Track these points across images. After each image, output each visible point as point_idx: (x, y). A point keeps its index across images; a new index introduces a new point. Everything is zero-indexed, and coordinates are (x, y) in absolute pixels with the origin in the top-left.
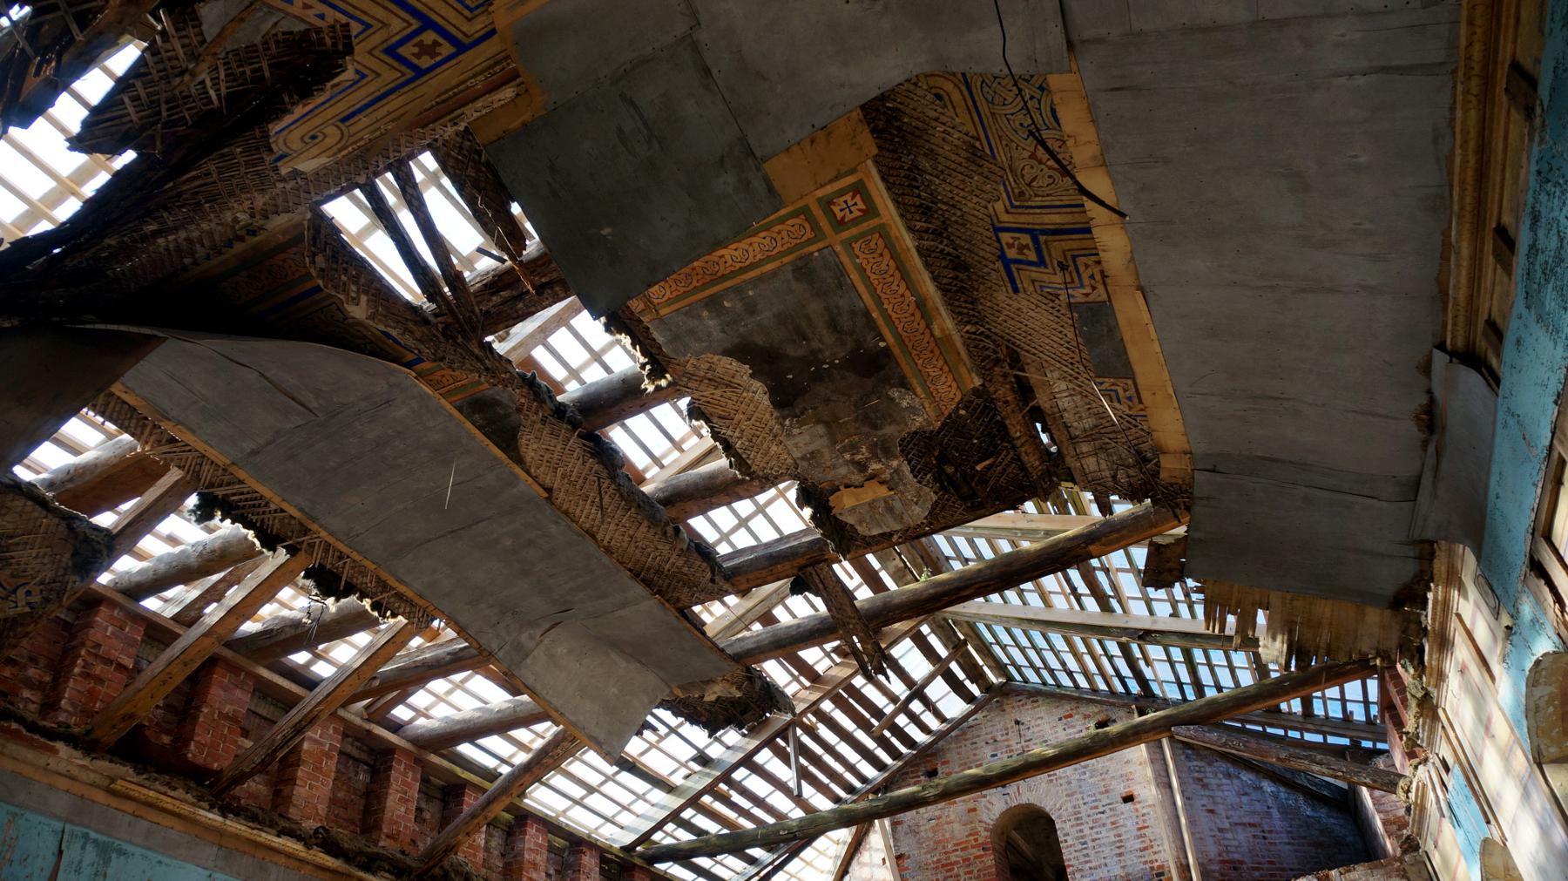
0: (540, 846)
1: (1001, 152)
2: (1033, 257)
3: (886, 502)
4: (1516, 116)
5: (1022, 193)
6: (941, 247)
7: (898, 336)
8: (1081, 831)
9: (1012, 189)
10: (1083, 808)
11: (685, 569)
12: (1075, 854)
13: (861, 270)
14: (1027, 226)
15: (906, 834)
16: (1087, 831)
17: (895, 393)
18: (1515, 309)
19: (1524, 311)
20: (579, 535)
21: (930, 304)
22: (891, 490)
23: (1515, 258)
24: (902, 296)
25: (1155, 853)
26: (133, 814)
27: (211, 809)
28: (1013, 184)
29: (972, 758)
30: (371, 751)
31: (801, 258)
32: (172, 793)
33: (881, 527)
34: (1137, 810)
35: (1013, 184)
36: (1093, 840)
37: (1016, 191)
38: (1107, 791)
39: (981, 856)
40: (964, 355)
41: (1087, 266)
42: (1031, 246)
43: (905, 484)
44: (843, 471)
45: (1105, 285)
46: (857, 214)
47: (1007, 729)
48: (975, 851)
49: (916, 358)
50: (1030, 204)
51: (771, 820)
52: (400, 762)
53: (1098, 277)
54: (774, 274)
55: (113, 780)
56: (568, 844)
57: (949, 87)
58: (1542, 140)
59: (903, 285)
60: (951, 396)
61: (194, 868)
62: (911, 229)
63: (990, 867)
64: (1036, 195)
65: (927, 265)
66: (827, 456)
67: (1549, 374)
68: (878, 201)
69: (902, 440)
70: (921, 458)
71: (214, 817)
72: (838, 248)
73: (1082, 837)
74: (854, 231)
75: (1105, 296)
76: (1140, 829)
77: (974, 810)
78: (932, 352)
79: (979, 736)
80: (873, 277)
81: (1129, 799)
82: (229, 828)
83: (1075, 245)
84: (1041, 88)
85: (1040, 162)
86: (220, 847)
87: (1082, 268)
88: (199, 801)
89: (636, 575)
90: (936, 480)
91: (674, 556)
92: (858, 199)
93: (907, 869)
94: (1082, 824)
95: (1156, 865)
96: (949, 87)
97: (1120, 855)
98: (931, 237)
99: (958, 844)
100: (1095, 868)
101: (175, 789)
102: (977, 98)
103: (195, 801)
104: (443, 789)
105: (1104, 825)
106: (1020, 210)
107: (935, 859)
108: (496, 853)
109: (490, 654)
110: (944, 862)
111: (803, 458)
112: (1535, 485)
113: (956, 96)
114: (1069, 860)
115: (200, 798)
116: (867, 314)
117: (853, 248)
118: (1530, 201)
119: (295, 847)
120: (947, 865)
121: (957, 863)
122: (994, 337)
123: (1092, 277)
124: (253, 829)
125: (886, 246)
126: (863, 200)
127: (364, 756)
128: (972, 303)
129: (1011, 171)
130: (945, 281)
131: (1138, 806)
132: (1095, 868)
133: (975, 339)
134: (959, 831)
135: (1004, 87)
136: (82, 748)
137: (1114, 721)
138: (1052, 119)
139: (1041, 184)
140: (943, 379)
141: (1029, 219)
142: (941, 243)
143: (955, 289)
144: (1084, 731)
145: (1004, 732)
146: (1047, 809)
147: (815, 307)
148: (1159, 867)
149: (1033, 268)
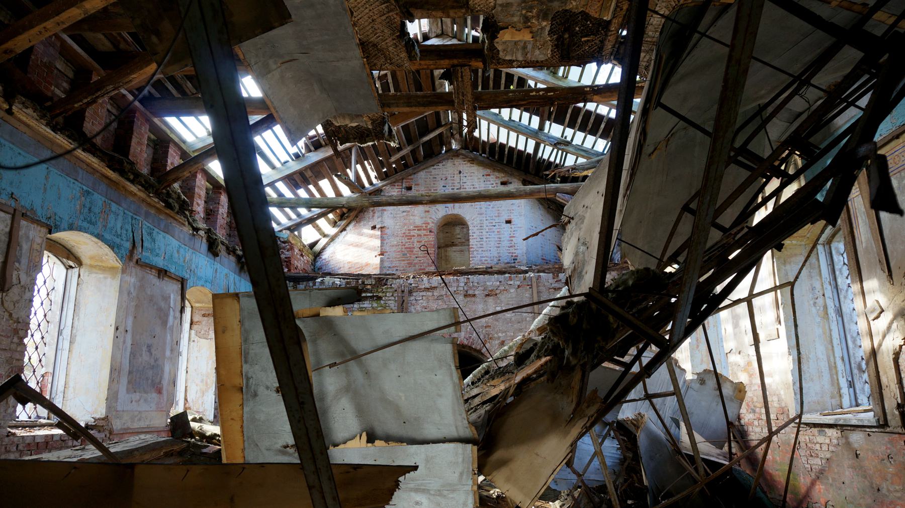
3: (525, 43)
8: (482, 232)
10: (485, 222)
11: (390, 49)
12: (476, 243)
16: (484, 233)
20: (344, 9)
22: (532, 38)
25: (515, 249)
27: (47, 125)
29: (432, 185)
30: (118, 108)
32: (25, 110)
33: (513, 56)
34: (511, 228)
36: (487, 238)
38: (499, 216)
39: (428, 235)
43: (541, 37)
44: (515, 19)
47: (454, 174)
48: (425, 232)
51: (318, 195)
52: (138, 120)
56: (211, 187)
63: (432, 241)
66: (514, 8)
69: (556, 13)
70: (559, 25)
73: (481, 236)
76: (511, 237)
77: (428, 212)
79: (438, 175)
81: (509, 222)
82: (57, 140)
88: (41, 119)
89: (363, 45)
90: (557, 39)
91: (390, 39)
93: (386, 234)
94: (482, 229)
95: (514, 255)
97: (499, 247)
99: (416, 227)
100: (484, 251)
101: (27, 108)
103: (38, 118)
104: (153, 141)
105: (494, 232)
107: (402, 232)
109: (249, 65)
110: (407, 234)
111: (501, 5)
114: (473, 245)
119: (94, 160)
120: (409, 236)
121: (414, 236)
124: (71, 144)
127: (114, 111)
131: (512, 226)
132: (484, 251)
134: (418, 221)
137: (511, 183)
144: (495, 185)
145: (452, 176)
146: (467, 219)
148: (515, 256)
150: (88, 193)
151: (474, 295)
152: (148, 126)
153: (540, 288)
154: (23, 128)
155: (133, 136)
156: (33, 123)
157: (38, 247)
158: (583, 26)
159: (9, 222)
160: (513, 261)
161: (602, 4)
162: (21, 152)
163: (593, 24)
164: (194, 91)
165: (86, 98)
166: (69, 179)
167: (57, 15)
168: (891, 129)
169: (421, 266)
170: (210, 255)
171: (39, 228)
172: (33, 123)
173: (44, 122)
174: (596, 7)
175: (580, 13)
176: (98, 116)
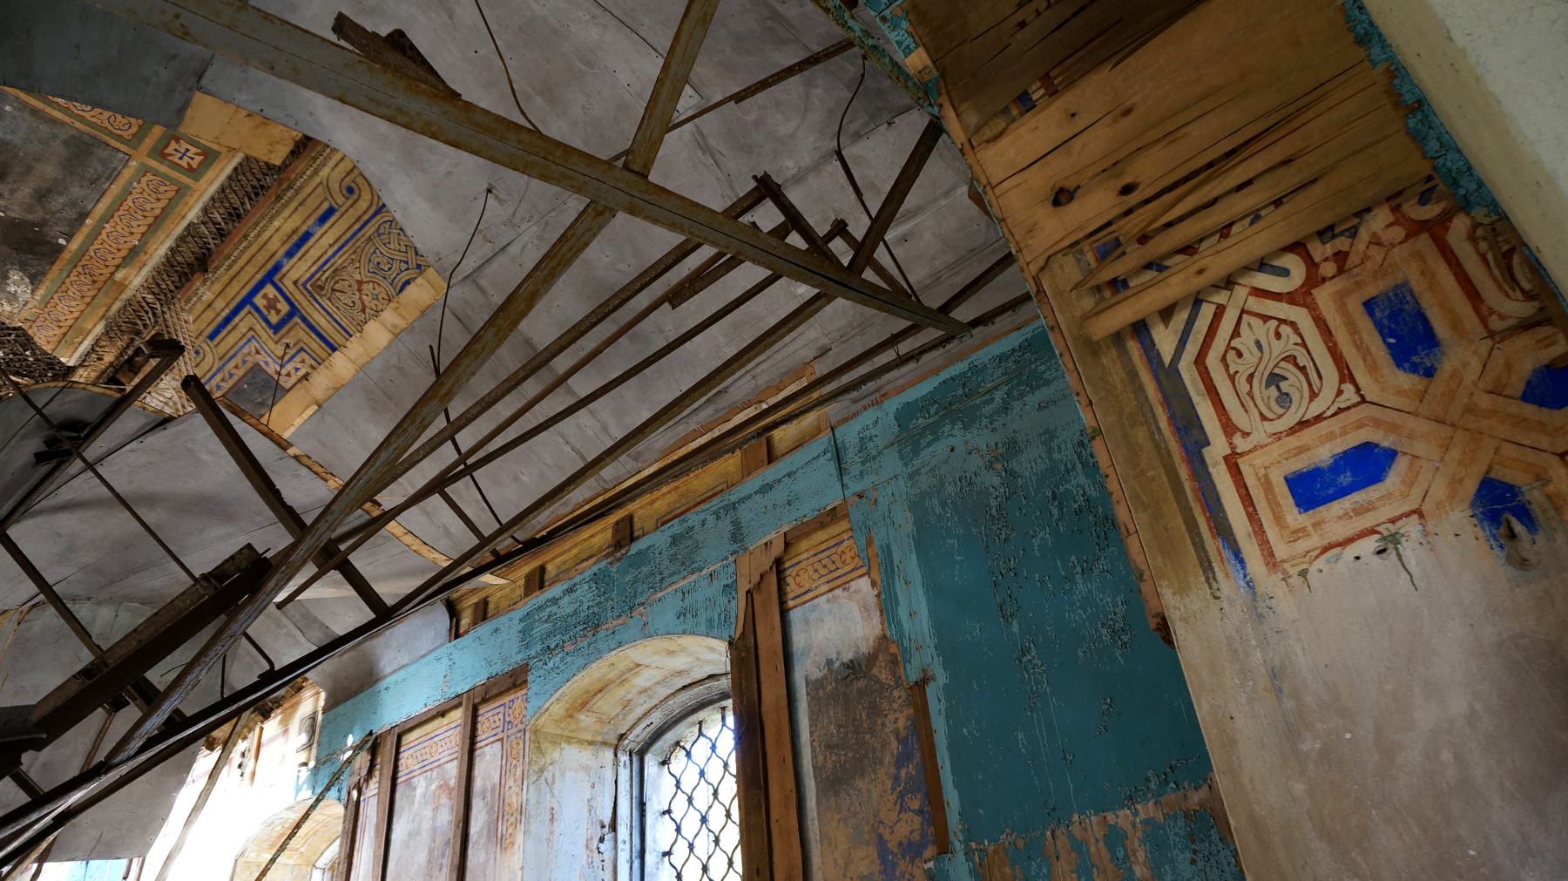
1: (344, 258)
2: (274, 319)
4: (609, 534)
5: (322, 288)
6: (211, 241)
7: (83, 251)
9: (319, 279)
13: (127, 192)
14: (296, 304)
17: (15, 276)
18: (513, 613)
19: (516, 621)
21: (143, 258)
23: (538, 593)
24: (132, 233)
28: (323, 278)
31: (95, 138)
35: (323, 278)
37: (320, 283)
40: (118, 305)
41: (303, 361)
42: (283, 313)
45: (300, 381)
46: (184, 163)
49: (75, 273)
50: (318, 297)
53: (301, 373)
54: (54, 121)
57: (366, 196)
58: (611, 563)
59: (143, 229)
60: (62, 318)
62: (205, 211)
64: (329, 299)
65: (182, 239)
67: (500, 661)
68: (210, 174)
72: (133, 164)
74: (164, 169)
75: (288, 386)
78: (94, 282)
80: (129, 202)
83: (314, 346)
84: (419, 267)
85: (360, 290)
87: (298, 359)
92: (198, 159)
96: (366, 196)
98: (215, 230)
102: (373, 221)
106: (304, 292)
112: (426, 706)
113: (363, 205)
116: (84, 215)
117: (144, 175)
118: (578, 579)
122: (161, 320)
123: (297, 369)
125: (170, 199)
126: (200, 164)
128: (176, 287)
129: (334, 272)
130: (179, 259)
133: (141, 306)
135: (399, 239)
138: (400, 284)
139: (342, 298)
140: (74, 303)
141: (305, 303)
142: (213, 239)
143: (179, 268)
147: (49, 170)
149: (264, 324)
158: (15, 354)
161: (65, 334)
163: (37, 360)
168: (439, 700)
174: (51, 333)
175: (14, 329)
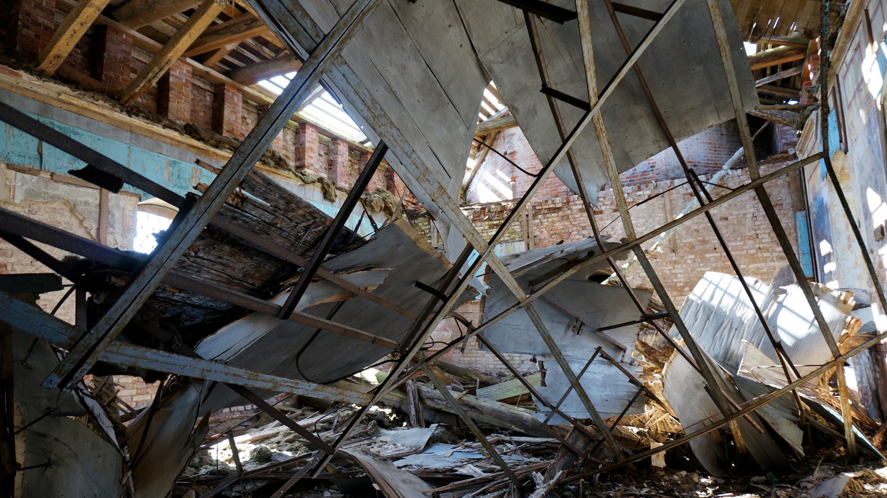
0: (314, 139)
15: (517, 140)
26: (77, 113)
27: (122, 111)
30: (211, 84)
32: (97, 103)
52: (229, 91)
55: (59, 94)
61: (118, 143)
71: (124, 117)
86: (132, 132)
101: (97, 100)
104: (256, 107)
108: (290, 143)
115: (114, 106)
127: (208, 88)
136: (35, 75)
148: (653, 163)
150: (175, 162)
151: (601, 212)
152: (241, 95)
153: (674, 195)
154: (98, 117)
155: (225, 107)
156: (106, 112)
157: (131, 214)
159: (98, 196)
160: (651, 169)
162: (100, 138)
164: (273, 55)
165: (142, 82)
166: (152, 153)
167: (77, 17)
169: (552, 187)
170: (328, 203)
171: (129, 198)
172: (106, 112)
173: (118, 109)
176: (183, 95)
